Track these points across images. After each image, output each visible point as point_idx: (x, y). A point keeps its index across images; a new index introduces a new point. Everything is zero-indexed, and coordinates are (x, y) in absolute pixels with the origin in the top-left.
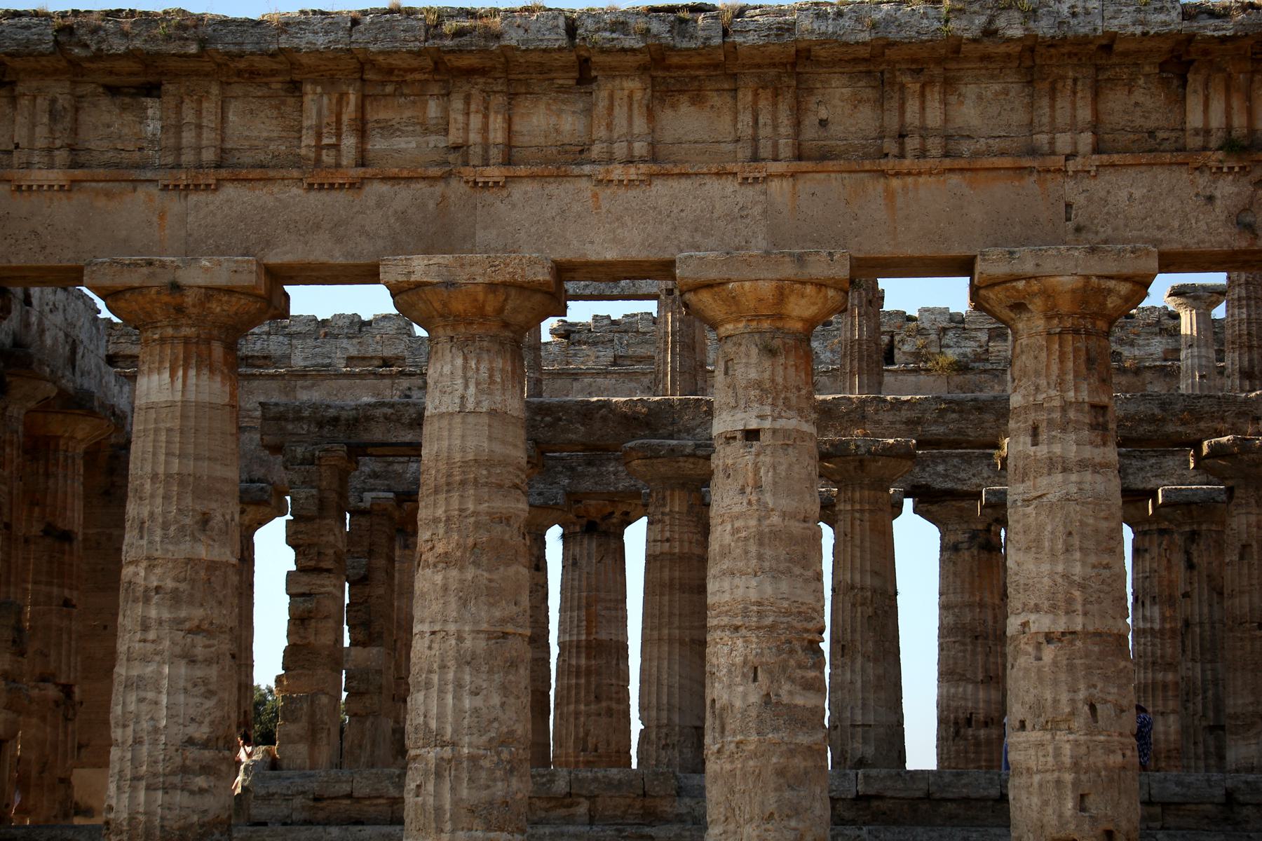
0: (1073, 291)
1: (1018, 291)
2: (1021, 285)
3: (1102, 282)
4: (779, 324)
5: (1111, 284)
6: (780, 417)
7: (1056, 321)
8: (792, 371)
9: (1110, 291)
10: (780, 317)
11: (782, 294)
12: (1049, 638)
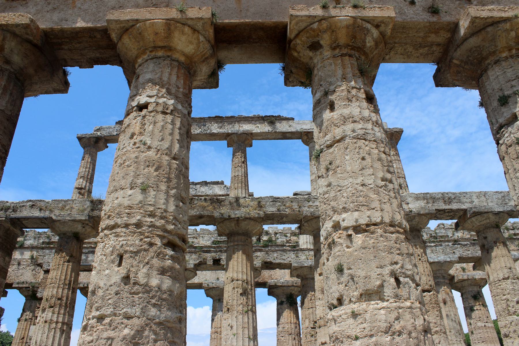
0: (347, 27)
1: (314, 30)
2: (315, 26)
3: (364, 22)
4: (169, 54)
5: (369, 26)
6: (163, 96)
7: (337, 51)
8: (174, 78)
9: (368, 30)
10: (169, 48)
11: (169, 29)
12: (358, 229)
